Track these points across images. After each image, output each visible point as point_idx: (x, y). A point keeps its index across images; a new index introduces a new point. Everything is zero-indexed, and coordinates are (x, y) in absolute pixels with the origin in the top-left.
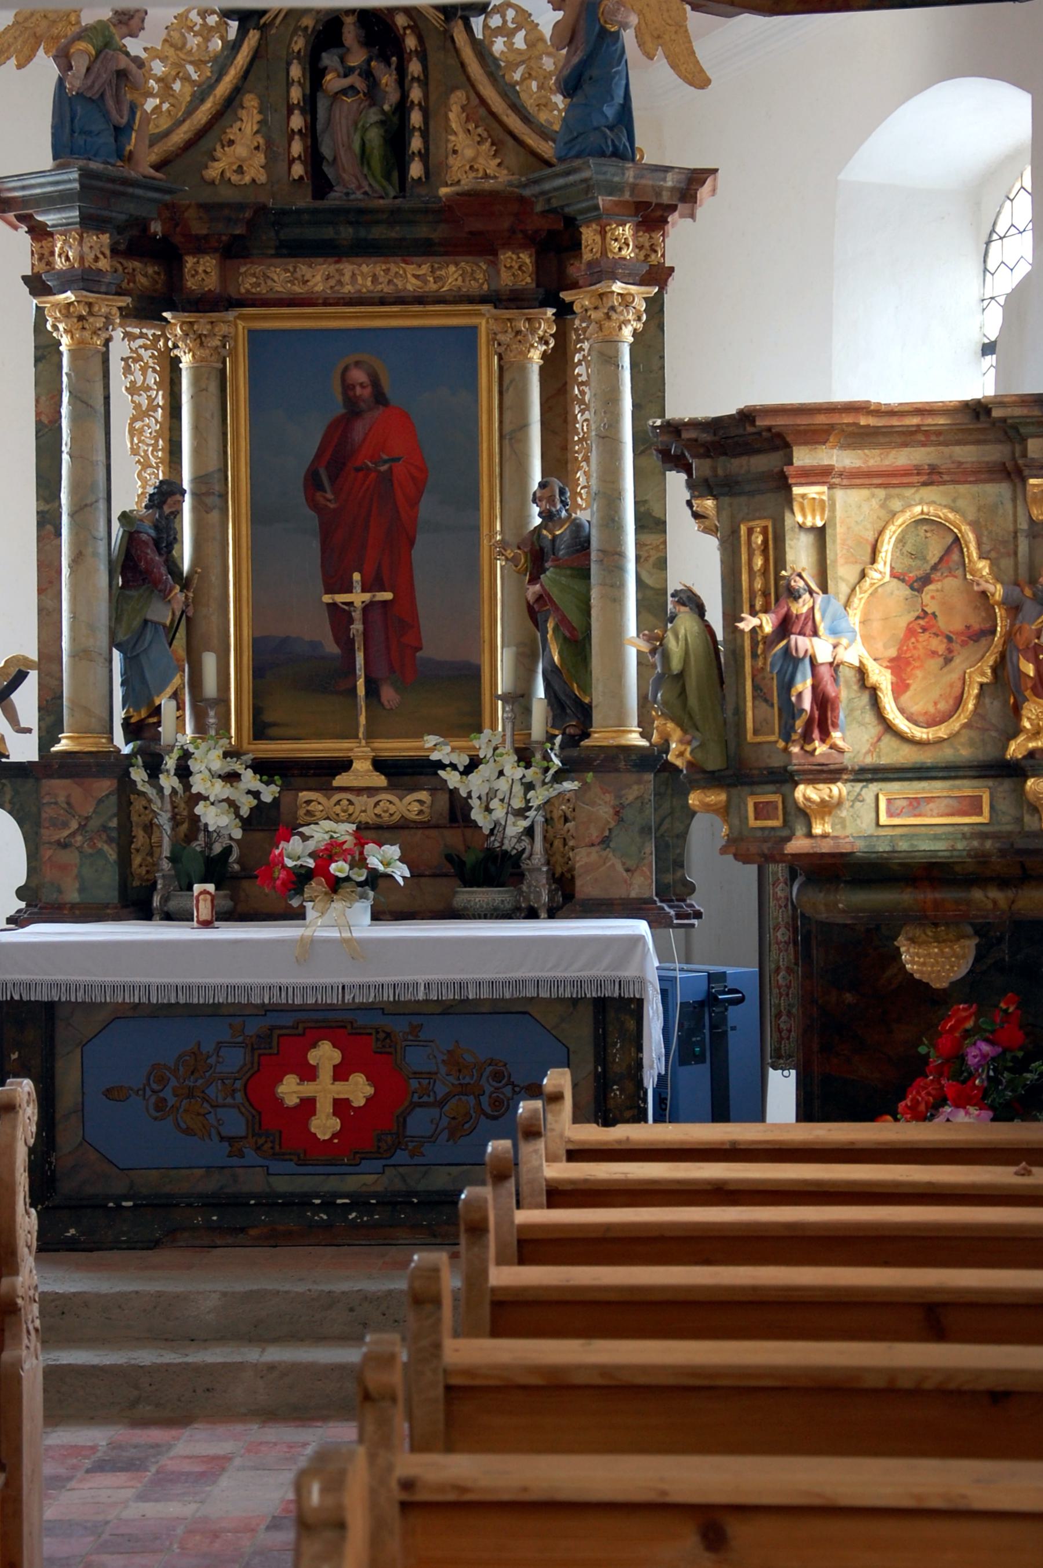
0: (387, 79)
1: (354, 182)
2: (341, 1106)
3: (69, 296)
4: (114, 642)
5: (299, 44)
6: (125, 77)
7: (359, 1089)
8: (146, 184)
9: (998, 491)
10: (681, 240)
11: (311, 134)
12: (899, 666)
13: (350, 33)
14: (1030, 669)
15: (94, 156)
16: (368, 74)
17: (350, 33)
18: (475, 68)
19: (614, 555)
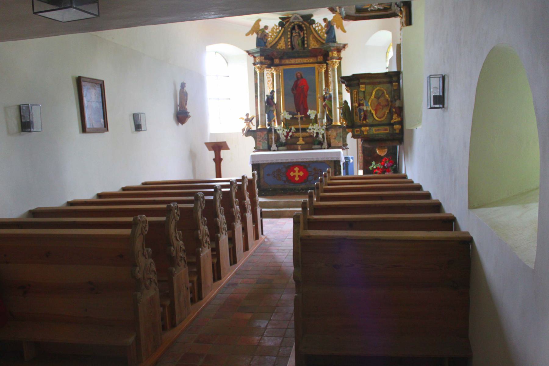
0: (302, 34)
1: (298, 48)
2: (299, 176)
3: (259, 65)
4: (266, 113)
5: (289, 29)
6: (266, 35)
7: (301, 174)
8: (269, 49)
9: (389, 85)
10: (343, 54)
11: (291, 42)
12: (376, 110)
13: (296, 27)
14: (394, 110)
15: (261, 46)
16: (299, 33)
17: (296, 27)
18: (314, 32)
19: (335, 98)
